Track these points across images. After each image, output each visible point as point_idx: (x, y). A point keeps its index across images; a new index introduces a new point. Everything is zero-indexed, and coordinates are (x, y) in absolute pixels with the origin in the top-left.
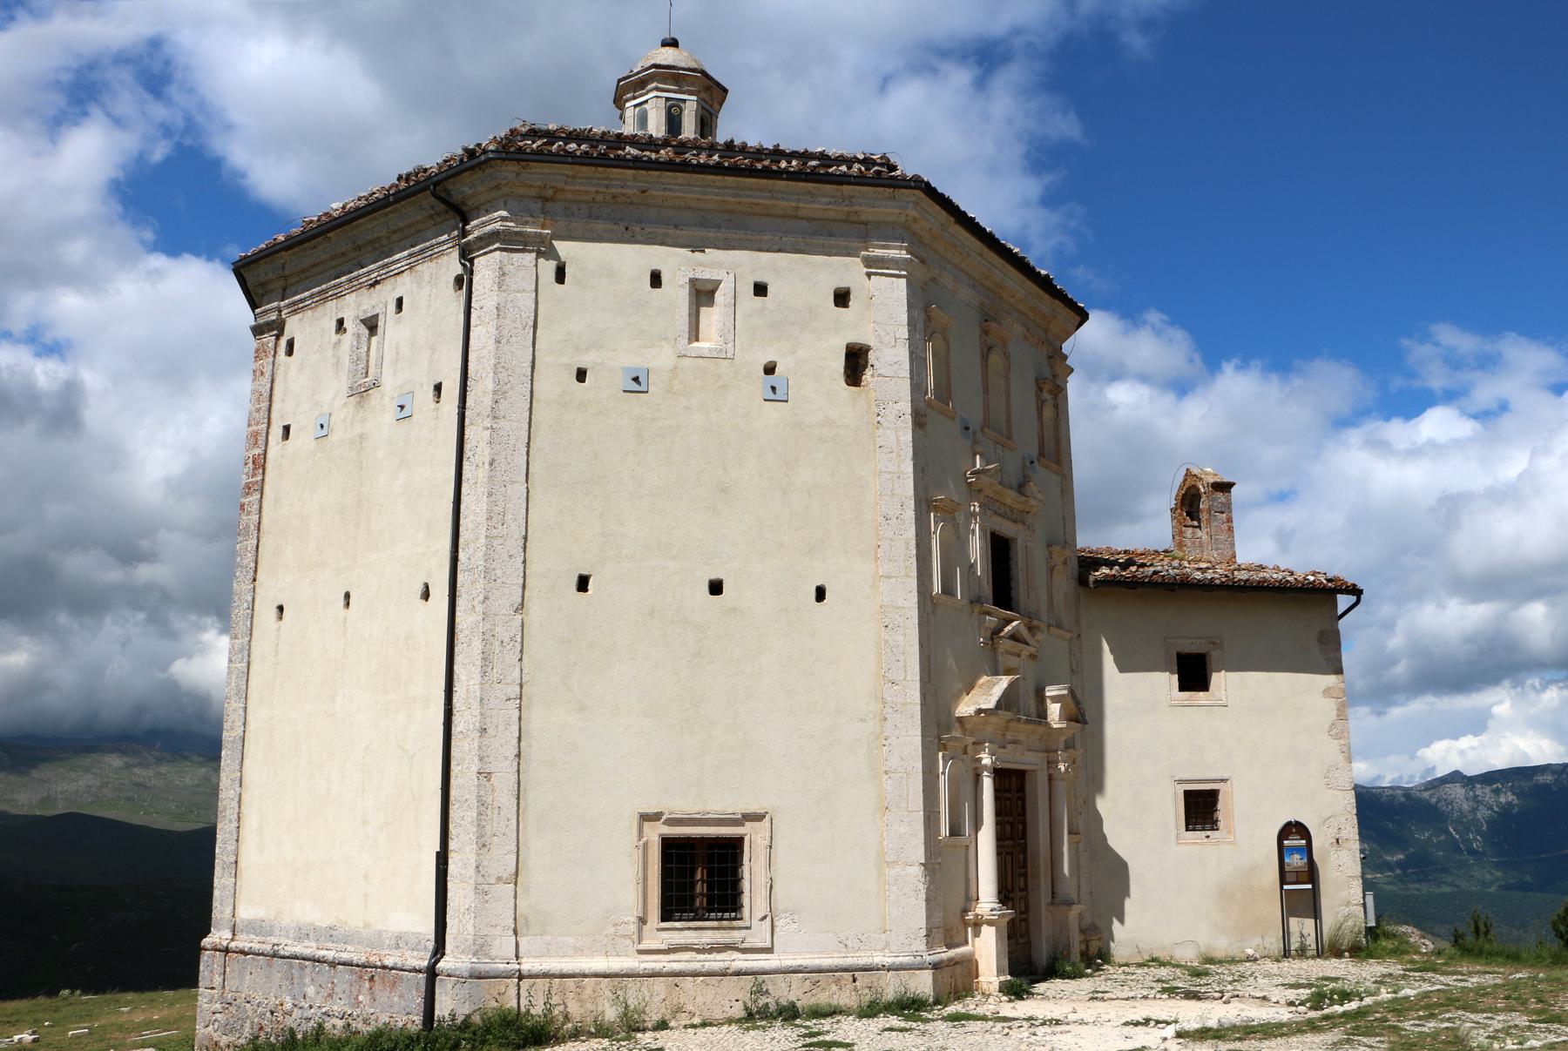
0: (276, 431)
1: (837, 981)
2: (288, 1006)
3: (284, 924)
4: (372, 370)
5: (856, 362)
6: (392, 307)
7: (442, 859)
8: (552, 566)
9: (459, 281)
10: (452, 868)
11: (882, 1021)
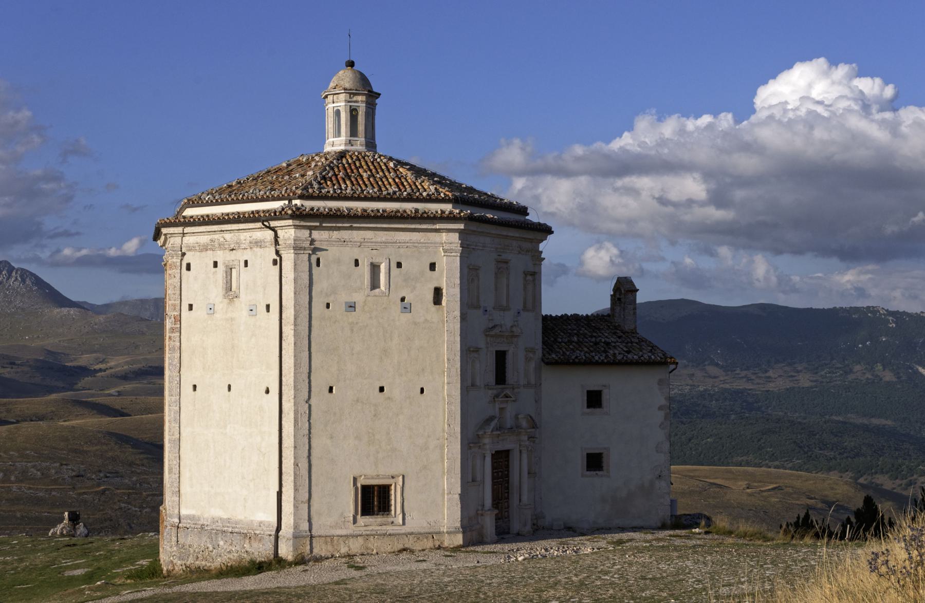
0: (185, 307)
1: (427, 538)
2: (211, 549)
3: (205, 516)
4: (234, 288)
5: (438, 292)
6: (242, 264)
7: (280, 494)
8: (320, 382)
9: (275, 262)
10: (284, 497)
11: (442, 552)
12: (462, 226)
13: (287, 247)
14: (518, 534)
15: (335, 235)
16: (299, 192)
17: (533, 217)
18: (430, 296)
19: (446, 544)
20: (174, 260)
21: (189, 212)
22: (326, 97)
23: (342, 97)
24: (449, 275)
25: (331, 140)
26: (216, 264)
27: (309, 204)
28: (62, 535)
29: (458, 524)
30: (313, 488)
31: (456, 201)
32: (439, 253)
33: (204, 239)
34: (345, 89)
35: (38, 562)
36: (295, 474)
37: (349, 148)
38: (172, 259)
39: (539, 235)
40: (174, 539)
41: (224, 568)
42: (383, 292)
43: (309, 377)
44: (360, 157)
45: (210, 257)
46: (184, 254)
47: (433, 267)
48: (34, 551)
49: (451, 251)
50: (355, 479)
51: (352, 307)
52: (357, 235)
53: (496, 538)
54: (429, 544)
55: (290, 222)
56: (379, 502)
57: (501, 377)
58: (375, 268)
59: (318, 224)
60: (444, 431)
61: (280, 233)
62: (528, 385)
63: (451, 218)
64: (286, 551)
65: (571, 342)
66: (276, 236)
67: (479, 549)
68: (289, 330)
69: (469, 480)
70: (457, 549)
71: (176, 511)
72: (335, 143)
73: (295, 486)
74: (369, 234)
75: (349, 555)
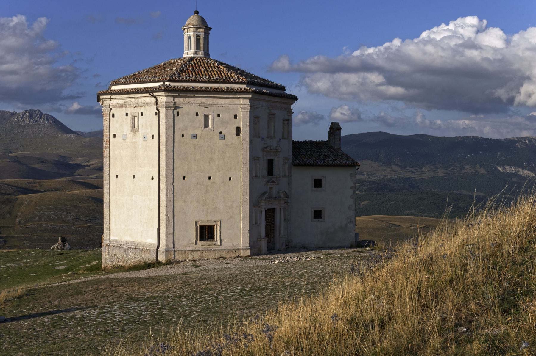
0: (112, 136)
3: (123, 240)
4: (136, 127)
5: (238, 130)
6: (140, 114)
8: (179, 174)
9: (156, 114)
10: (161, 231)
11: (240, 259)
12: (250, 96)
13: (162, 106)
14: (279, 250)
15: (187, 100)
16: (168, 78)
17: (288, 92)
18: (234, 131)
19: (242, 255)
20: (106, 112)
21: (114, 88)
22: (184, 29)
23: (192, 29)
24: (244, 121)
25: (186, 51)
26: (127, 114)
27: (173, 84)
28: (58, 249)
29: (248, 245)
30: (175, 227)
31: (247, 83)
32: (239, 109)
33: (121, 102)
34: (193, 26)
35: (43, 262)
36: (166, 220)
37: (196, 56)
38: (106, 112)
39: (290, 101)
40: (107, 251)
41: (132, 266)
42: (210, 129)
43: (173, 172)
44: (201, 60)
45: (124, 111)
46: (111, 109)
47: (236, 117)
48: (42, 257)
49: (245, 108)
50: (196, 223)
51: (195, 136)
52: (197, 100)
53: (267, 252)
54: (233, 255)
55: (163, 93)
56: (209, 234)
57: (270, 172)
58: (206, 117)
59: (177, 95)
60: (241, 199)
61: (158, 99)
62: (285, 176)
63: (245, 92)
64: (162, 258)
65: (307, 154)
66: (157, 100)
67: (258, 257)
68: (163, 148)
69: (253, 223)
70: (247, 257)
71: (108, 238)
72: (189, 53)
73: (166, 226)
74: (203, 100)
75: (193, 260)
